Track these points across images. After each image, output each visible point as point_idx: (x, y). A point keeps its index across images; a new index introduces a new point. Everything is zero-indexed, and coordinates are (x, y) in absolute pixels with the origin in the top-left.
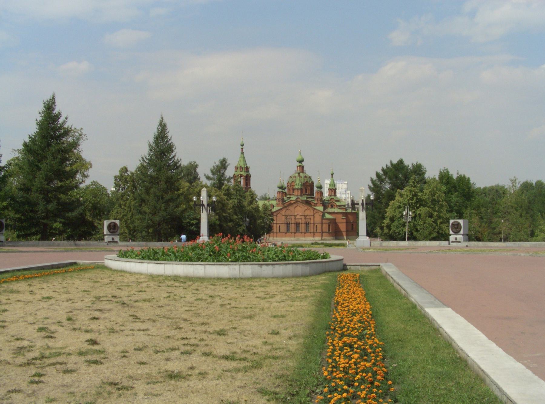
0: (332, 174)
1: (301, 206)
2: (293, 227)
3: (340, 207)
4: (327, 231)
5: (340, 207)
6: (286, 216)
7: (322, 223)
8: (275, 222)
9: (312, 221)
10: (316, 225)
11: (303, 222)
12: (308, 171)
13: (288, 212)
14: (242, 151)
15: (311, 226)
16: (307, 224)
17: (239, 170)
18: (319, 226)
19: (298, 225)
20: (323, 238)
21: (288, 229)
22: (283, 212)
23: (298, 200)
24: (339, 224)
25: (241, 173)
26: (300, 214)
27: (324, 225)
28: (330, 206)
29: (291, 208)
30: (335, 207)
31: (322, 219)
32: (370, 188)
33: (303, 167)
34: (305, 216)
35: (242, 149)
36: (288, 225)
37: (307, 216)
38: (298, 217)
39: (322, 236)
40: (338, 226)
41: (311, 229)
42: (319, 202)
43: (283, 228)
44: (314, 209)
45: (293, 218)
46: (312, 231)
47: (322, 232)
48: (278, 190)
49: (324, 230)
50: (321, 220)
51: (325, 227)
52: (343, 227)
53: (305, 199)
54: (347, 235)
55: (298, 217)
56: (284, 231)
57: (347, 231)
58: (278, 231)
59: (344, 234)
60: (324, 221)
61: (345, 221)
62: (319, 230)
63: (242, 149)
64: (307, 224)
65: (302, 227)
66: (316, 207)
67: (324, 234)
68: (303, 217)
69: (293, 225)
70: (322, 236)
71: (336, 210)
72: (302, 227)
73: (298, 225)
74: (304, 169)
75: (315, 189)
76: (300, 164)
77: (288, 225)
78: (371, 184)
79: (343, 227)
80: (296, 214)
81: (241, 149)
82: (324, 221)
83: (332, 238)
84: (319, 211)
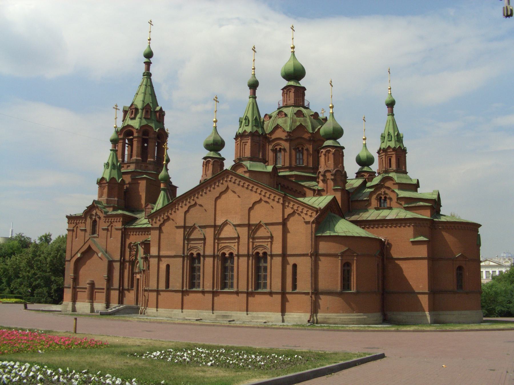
0: (391, 105)
1: (238, 189)
3: (410, 203)
4: (339, 290)
5: (410, 203)
6: (188, 230)
7: (315, 255)
9: (277, 249)
10: (291, 261)
12: (316, 98)
14: (148, 69)
16: (259, 260)
18: (305, 266)
19: (225, 261)
20: (320, 316)
21: (193, 279)
24: (403, 265)
27: (324, 263)
28: (374, 202)
30: (394, 203)
31: (317, 239)
34: (253, 229)
35: (148, 64)
37: (259, 226)
38: (228, 232)
40: (400, 270)
42: (331, 183)
45: (210, 233)
46: (277, 286)
47: (316, 293)
49: (322, 286)
51: (330, 273)
52: (417, 275)
54: (433, 308)
56: (178, 287)
57: (434, 292)
59: (424, 300)
60: (324, 247)
61: (423, 251)
62: (304, 284)
63: (148, 64)
64: (259, 260)
67: (324, 300)
68: (244, 232)
71: (397, 213)
73: (225, 261)
77: (193, 261)
79: (417, 275)
81: (144, 66)
82: (324, 247)
83: (362, 316)
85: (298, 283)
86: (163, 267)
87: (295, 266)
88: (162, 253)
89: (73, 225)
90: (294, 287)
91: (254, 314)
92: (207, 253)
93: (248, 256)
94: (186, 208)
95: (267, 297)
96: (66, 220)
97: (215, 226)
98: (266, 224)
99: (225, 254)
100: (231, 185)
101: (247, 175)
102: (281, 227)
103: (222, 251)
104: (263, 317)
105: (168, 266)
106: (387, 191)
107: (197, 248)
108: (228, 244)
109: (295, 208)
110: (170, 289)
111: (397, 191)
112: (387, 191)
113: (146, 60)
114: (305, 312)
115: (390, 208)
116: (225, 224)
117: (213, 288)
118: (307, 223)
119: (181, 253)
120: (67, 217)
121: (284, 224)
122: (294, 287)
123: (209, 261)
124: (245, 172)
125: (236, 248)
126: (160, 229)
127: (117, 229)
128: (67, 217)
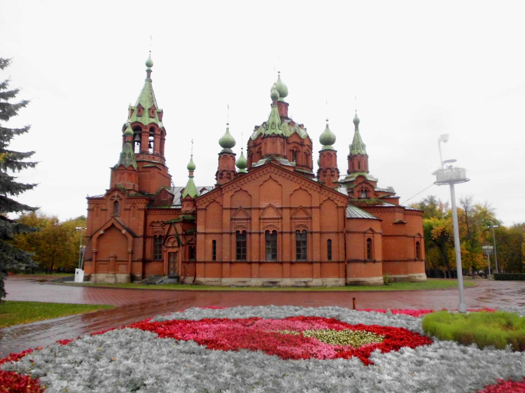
0: (356, 123)
1: (280, 180)
2: (255, 246)
11: (286, 229)
13: (241, 201)
14: (149, 76)
25: (139, 119)
26: (278, 205)
29: (251, 187)
35: (149, 72)
39: (346, 276)
43: (227, 249)
50: (341, 223)
55: (271, 214)
58: (209, 258)
63: (149, 72)
68: (286, 214)
69: (255, 237)
70: (346, 276)
73: (272, 238)
75: (317, 148)
80: (264, 205)
86: (210, 242)
87: (329, 241)
88: (208, 231)
89: (93, 206)
90: (330, 257)
92: (253, 231)
93: (291, 233)
94: (232, 193)
96: (86, 201)
97: (260, 209)
98: (305, 208)
99: (269, 232)
100: (273, 176)
105: (214, 242)
106: (367, 186)
107: (242, 226)
108: (272, 224)
110: (217, 260)
113: (146, 68)
114: (339, 277)
116: (270, 206)
117: (260, 259)
118: (338, 207)
119: (227, 230)
120: (89, 199)
122: (330, 257)
123: (255, 237)
125: (280, 226)
126: (205, 209)
127: (139, 210)
128: (89, 199)
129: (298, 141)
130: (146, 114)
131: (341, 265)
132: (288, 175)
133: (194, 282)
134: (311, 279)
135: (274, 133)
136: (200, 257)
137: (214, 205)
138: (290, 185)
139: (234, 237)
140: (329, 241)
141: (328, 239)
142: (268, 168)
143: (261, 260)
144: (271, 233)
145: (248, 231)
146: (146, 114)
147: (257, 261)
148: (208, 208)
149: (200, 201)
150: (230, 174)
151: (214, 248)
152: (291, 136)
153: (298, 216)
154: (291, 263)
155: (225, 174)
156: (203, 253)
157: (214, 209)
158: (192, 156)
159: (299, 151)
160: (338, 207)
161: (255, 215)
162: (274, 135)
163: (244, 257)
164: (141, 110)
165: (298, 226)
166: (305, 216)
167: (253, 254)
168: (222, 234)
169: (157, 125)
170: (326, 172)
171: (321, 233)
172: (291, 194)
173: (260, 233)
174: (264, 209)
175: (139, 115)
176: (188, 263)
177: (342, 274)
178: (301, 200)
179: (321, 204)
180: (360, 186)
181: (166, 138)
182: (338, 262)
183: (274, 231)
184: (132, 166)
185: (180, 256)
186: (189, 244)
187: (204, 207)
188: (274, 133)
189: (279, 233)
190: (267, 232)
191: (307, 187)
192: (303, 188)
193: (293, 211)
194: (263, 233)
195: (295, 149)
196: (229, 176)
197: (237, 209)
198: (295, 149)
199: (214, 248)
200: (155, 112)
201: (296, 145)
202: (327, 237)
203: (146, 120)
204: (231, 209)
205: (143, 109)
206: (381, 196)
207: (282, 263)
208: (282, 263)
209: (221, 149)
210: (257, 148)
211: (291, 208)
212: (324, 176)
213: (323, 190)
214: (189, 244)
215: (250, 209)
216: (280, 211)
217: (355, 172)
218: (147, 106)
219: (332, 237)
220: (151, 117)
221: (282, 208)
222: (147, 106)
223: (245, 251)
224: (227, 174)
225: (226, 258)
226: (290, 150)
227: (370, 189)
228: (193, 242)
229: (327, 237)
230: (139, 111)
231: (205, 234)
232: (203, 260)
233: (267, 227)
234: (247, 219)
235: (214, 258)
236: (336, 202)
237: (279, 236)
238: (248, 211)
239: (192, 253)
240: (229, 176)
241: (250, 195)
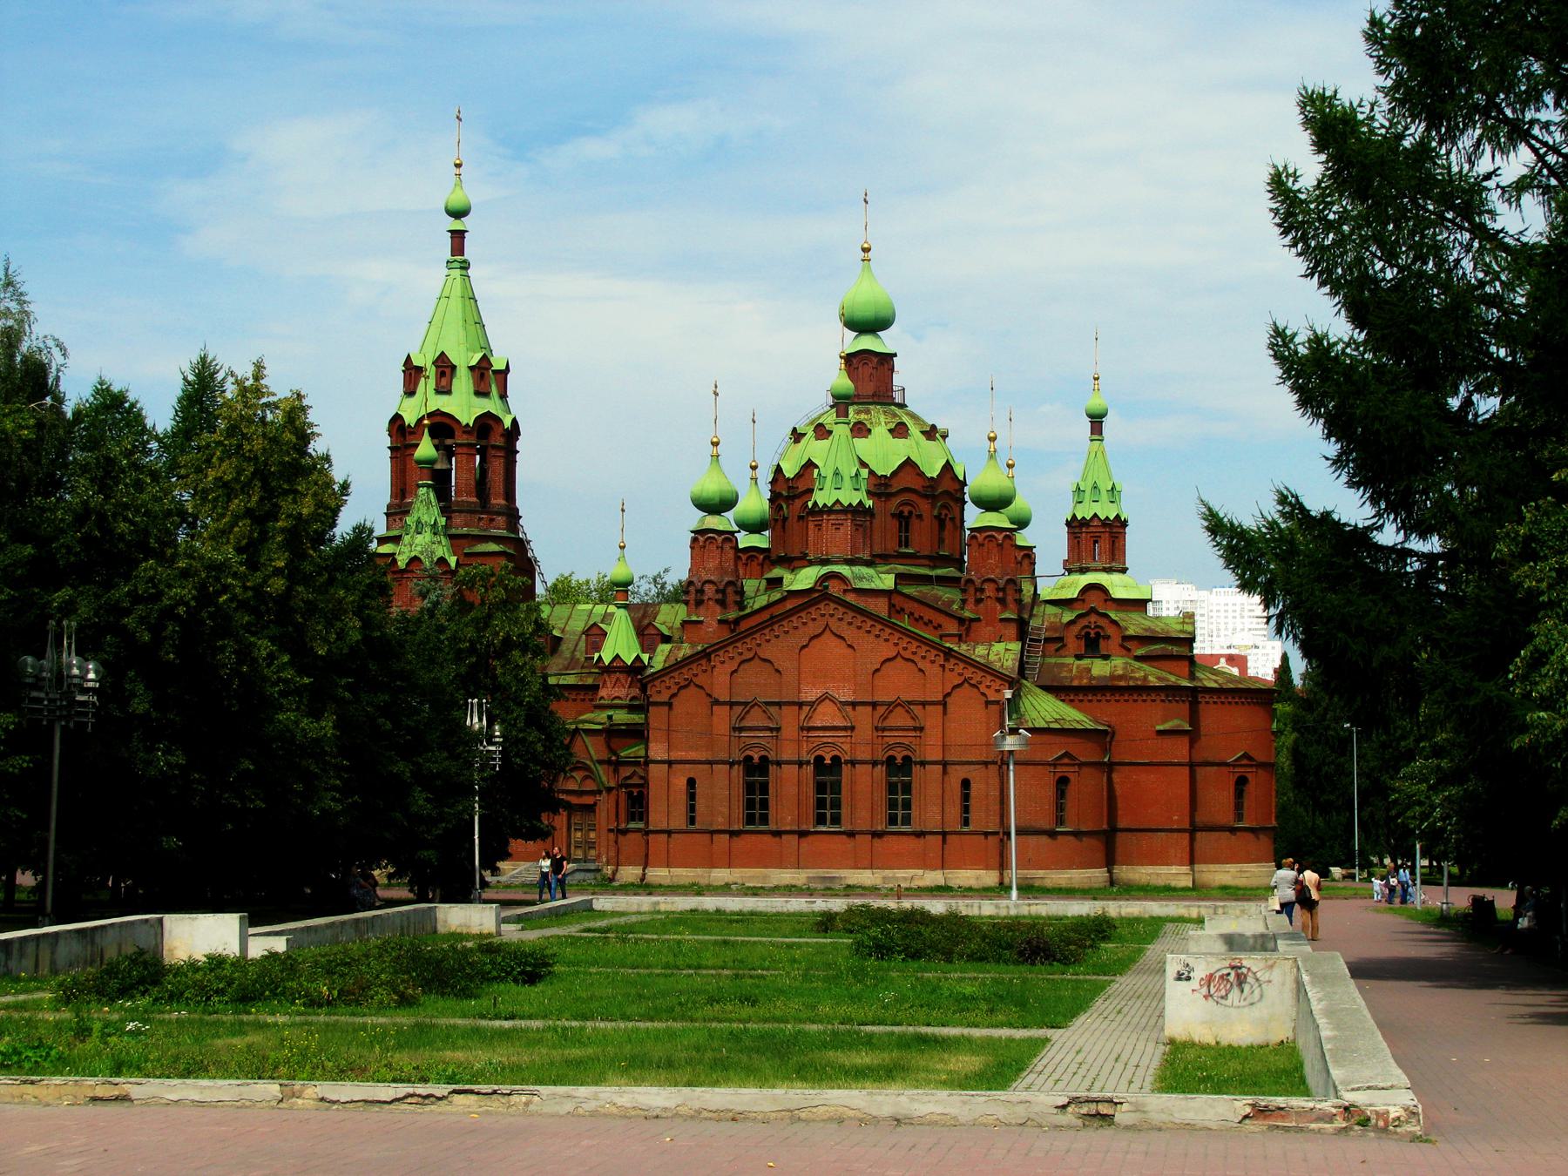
0: (1096, 422)
1: (848, 632)
2: (790, 791)
8: (658, 751)
13: (755, 683)
15: (926, 782)
16: (899, 769)
17: (427, 386)
19: (827, 772)
22: (719, 679)
23: (835, 589)
26: (845, 695)
29: (779, 648)
32: (1294, 213)
33: (887, 360)
35: (458, 237)
36: (756, 772)
41: (932, 803)
43: (722, 797)
44: (949, 653)
48: (697, 518)
53: (888, 582)
55: (826, 716)
58: (679, 822)
63: (458, 237)
64: (899, 769)
65: (863, 790)
66: (963, 648)
68: (864, 717)
72: (863, 790)
73: (827, 772)
74: (898, 380)
76: (867, 343)
77: (757, 775)
78: (1310, 168)
80: (810, 694)
81: (447, 240)
84: (986, 669)
85: (973, 816)
86: (680, 783)
87: (966, 784)
88: (675, 755)
90: (966, 822)
91: (888, 873)
92: (785, 757)
95: (912, 843)
97: (801, 705)
98: (910, 703)
101: (850, 598)
102: (940, 708)
103: (819, 753)
104: (905, 879)
105: (691, 783)
106: (1102, 622)
107: (758, 744)
109: (968, 674)
110: (697, 826)
111: (1113, 615)
112: (1102, 622)
114: (987, 868)
115: (1106, 657)
119: (723, 756)
121: (944, 704)
124: (845, 591)
126: (670, 705)
129: (916, 484)
130: (463, 383)
131: (992, 840)
132: (870, 623)
133: (642, 879)
134: (920, 872)
135: (838, 501)
136: (657, 819)
137: (692, 690)
138: (875, 648)
139: (738, 771)
140: (966, 784)
141: (964, 776)
142: (822, 606)
143: (804, 827)
144: (828, 761)
145: (772, 756)
146: (463, 383)
147: (795, 828)
148: (675, 702)
149: (657, 683)
150: (723, 592)
151: (692, 797)
152: (894, 473)
153: (889, 723)
154: (877, 835)
155: (710, 590)
156: (665, 810)
157: (690, 702)
158: (622, 548)
159: (920, 517)
160: (988, 703)
161: (789, 721)
162: (838, 507)
163: (764, 819)
164: (448, 371)
165: (890, 747)
166: (911, 723)
167: (784, 813)
168: (710, 763)
169: (498, 420)
170: (982, 590)
171: (945, 764)
172: (877, 670)
173: (800, 764)
174: (811, 704)
175: (444, 390)
176: (625, 832)
177: (995, 860)
178: (899, 683)
179: (949, 694)
180: (1084, 622)
181: (519, 445)
182: (986, 834)
183: (835, 759)
184: (442, 561)
185: (604, 814)
186: (627, 786)
187: (664, 697)
188: (838, 501)
189: (847, 762)
190: (819, 759)
191: (914, 653)
192: (907, 654)
193: (881, 710)
194: (808, 763)
195: (906, 509)
196: (720, 596)
197: (746, 704)
198: (906, 509)
199: (692, 797)
200: (489, 377)
201: (913, 497)
202: (957, 774)
203: (463, 406)
204: (732, 704)
205: (454, 368)
206: (1140, 652)
207: (851, 834)
208: (851, 834)
209: (697, 518)
210: (798, 503)
211: (874, 705)
212: (979, 601)
213: (953, 661)
214: (627, 786)
215: (779, 704)
216: (849, 709)
217: (1083, 571)
218: (464, 359)
219: (973, 773)
220: (478, 393)
221: (854, 705)
222: (464, 359)
223: (765, 804)
224: (717, 591)
225: (720, 822)
226: (893, 515)
227: (1111, 631)
228: (635, 781)
229: (957, 774)
230: (443, 374)
231: (670, 763)
232: (664, 826)
233: (818, 747)
234: (771, 730)
235: (692, 821)
236: (983, 688)
237: (846, 769)
238: (773, 709)
239: (637, 804)
240: (720, 596)
241: (778, 671)
